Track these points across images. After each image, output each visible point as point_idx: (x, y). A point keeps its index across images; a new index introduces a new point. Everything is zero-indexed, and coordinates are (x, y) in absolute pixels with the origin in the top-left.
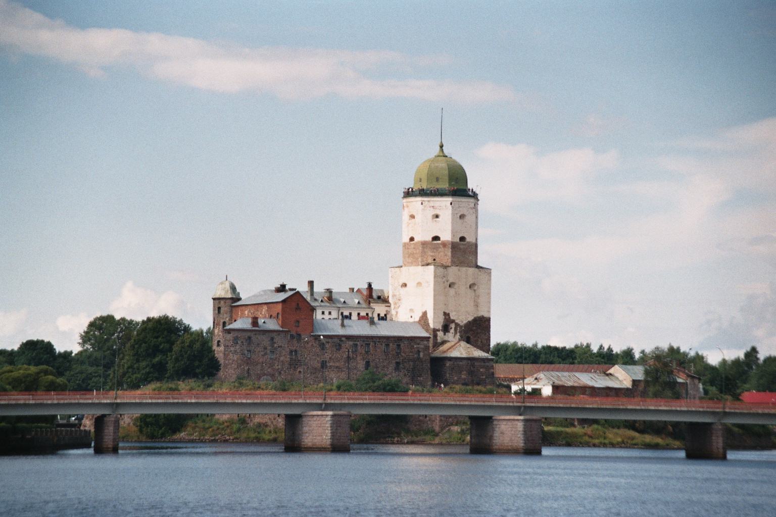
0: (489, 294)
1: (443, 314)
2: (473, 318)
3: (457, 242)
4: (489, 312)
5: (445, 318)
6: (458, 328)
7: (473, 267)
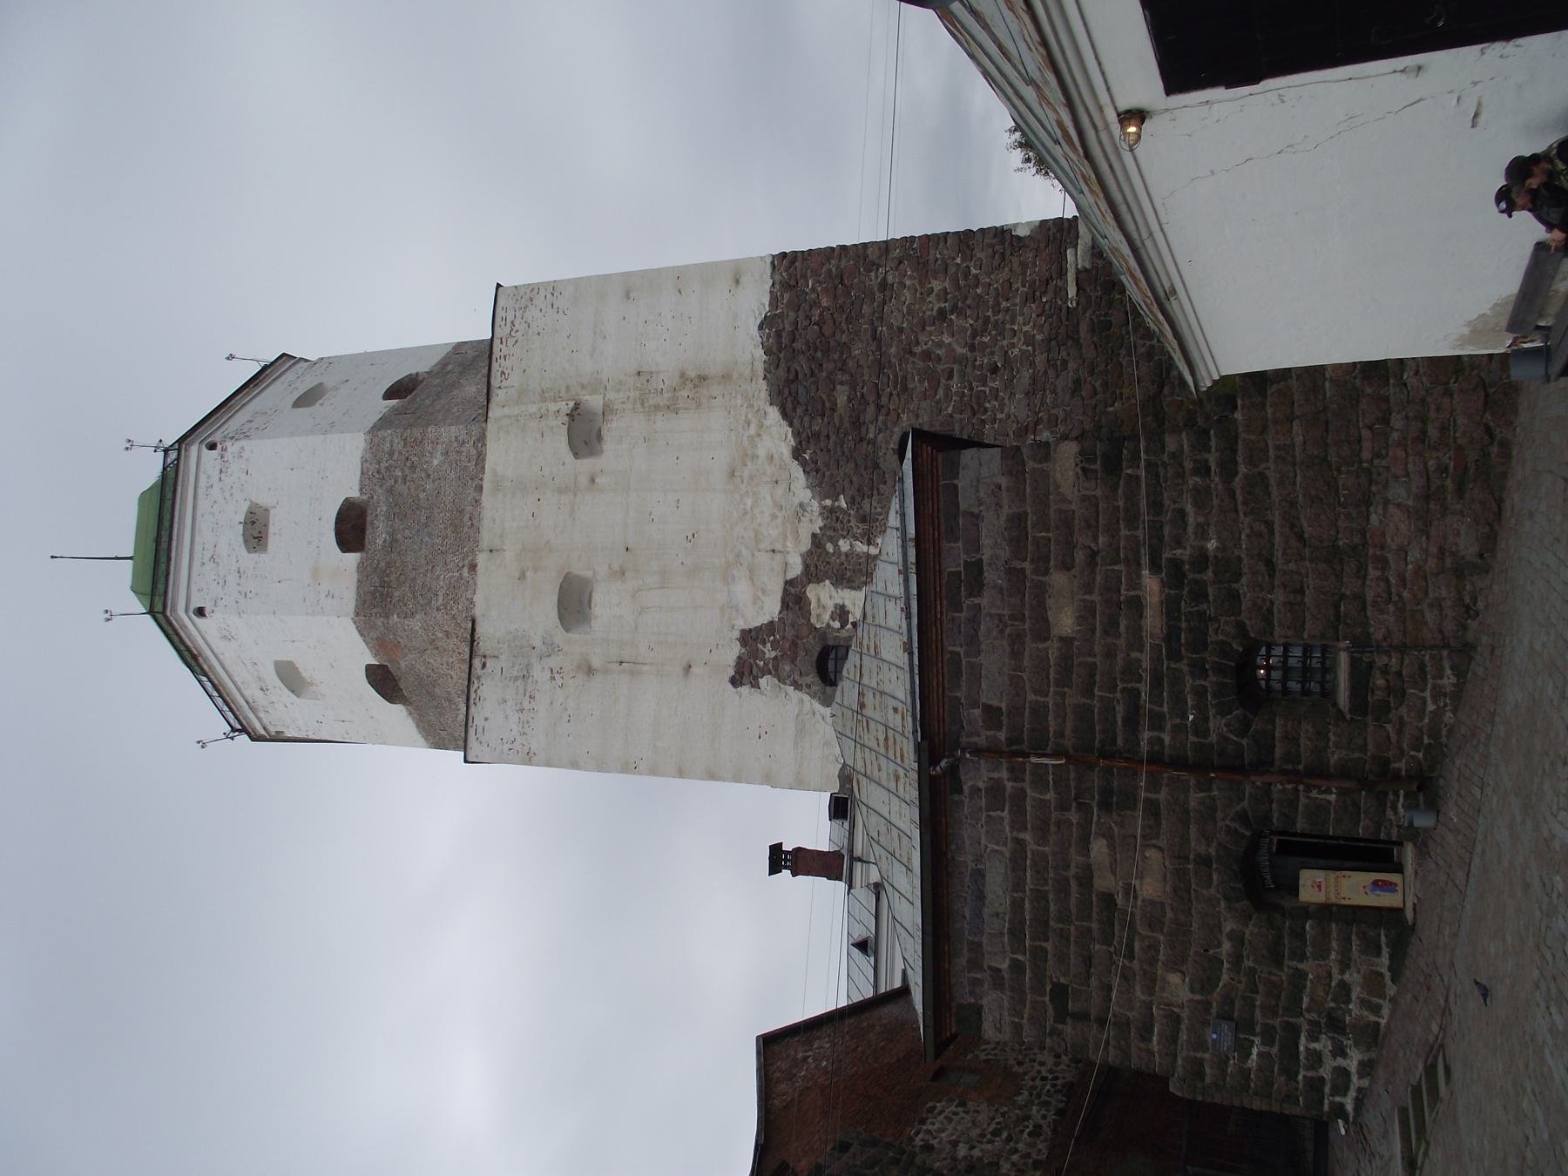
0: (630, 286)
1: (745, 690)
2: (774, 414)
3: (361, 568)
4: (736, 274)
5: (774, 669)
6: (844, 545)
7: (482, 438)
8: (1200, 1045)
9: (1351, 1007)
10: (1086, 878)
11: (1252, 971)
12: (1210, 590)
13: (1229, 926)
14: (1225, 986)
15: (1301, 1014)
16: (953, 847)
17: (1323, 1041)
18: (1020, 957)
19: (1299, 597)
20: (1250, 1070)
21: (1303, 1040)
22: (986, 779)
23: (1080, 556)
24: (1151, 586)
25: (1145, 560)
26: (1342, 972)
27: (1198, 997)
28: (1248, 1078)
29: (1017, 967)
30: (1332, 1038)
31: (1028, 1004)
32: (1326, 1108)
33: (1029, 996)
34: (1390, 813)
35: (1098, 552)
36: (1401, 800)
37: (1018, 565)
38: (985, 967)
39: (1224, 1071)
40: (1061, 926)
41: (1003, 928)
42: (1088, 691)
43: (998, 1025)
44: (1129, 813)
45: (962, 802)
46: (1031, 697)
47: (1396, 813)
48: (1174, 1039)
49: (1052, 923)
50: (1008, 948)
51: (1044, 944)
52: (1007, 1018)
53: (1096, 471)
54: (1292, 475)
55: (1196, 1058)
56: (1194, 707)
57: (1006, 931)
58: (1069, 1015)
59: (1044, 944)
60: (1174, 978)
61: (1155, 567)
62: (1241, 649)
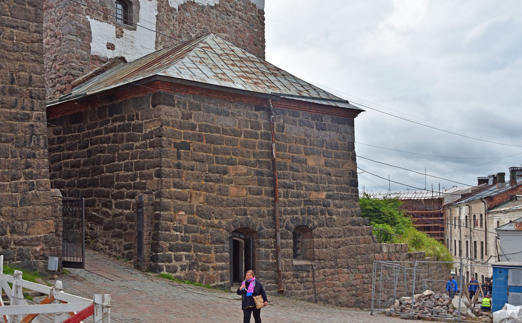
8: (177, 209)
9: (200, 271)
10: (232, 163)
11: (208, 232)
12: (323, 216)
13: (224, 222)
14: (201, 220)
15: (195, 252)
16: (236, 103)
17: (186, 261)
18: (197, 129)
19: (324, 247)
20: (170, 231)
21: (186, 253)
22: (261, 122)
23: (329, 169)
24: (323, 195)
25: (329, 193)
26: (213, 267)
27: (195, 209)
28: (166, 230)
29: (193, 127)
30: (187, 265)
31: (179, 130)
32: (160, 264)
33: (182, 131)
34: (268, 281)
35: (330, 176)
36: (272, 285)
37: (325, 145)
38: (192, 111)
39: (168, 220)
40: (212, 149)
41: (208, 122)
42: (292, 169)
43: (167, 114)
44: (257, 182)
45: (252, 110)
46: (288, 145)
47: (267, 283)
48: (177, 198)
49: (213, 145)
50: (200, 123)
51: (204, 141)
52: (171, 119)
53: (350, 177)
54: (353, 244)
56: (292, 209)
57: (207, 123)
58: (178, 150)
59: (204, 141)
60: (202, 199)
61: (328, 197)
62: (310, 227)
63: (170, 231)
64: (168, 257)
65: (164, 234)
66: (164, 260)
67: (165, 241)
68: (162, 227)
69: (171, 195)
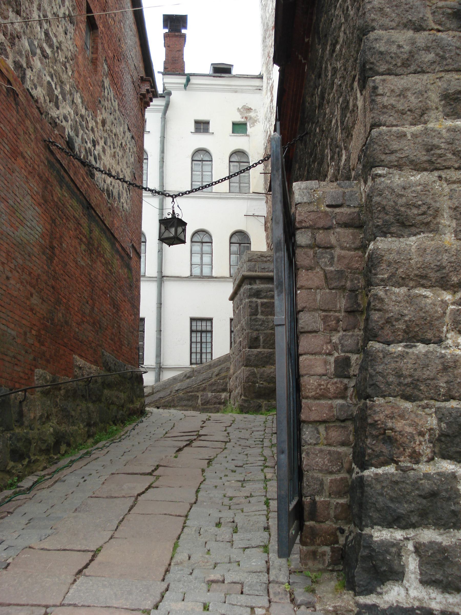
20: (439, 341)
55: (437, 212)
63: (439, 341)
64: (433, 495)
65: (402, 356)
66: (403, 508)
67: (408, 398)
68: (388, 321)
69: (430, 149)
